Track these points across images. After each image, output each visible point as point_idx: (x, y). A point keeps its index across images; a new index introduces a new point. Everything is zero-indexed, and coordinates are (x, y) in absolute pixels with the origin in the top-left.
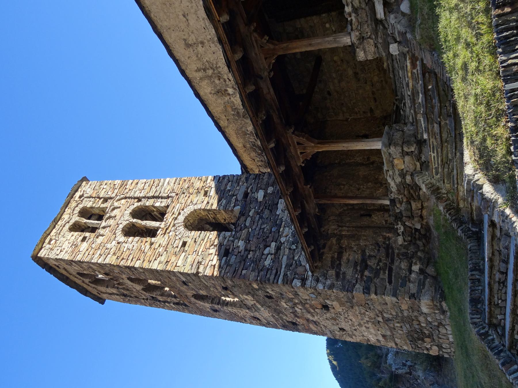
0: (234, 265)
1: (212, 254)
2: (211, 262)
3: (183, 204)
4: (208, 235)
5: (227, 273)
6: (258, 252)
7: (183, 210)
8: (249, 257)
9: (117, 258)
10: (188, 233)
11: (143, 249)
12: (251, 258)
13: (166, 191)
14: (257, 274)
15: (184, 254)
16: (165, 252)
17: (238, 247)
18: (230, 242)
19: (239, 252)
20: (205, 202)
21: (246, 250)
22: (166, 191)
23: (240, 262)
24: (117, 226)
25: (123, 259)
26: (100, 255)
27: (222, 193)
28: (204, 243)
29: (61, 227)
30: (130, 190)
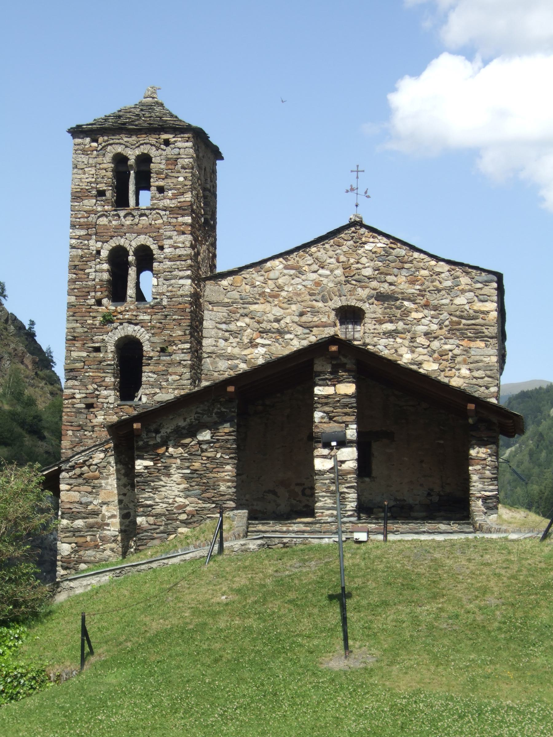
0: (76, 420)
1: (87, 389)
2: (77, 391)
3: (149, 324)
4: (109, 375)
5: (68, 416)
6: (91, 441)
7: (142, 327)
8: (86, 433)
9: (76, 266)
10: (111, 348)
11: (89, 297)
12: (85, 435)
13: (170, 288)
14: (68, 447)
15: (84, 354)
16: (86, 330)
17: (96, 416)
18: (101, 406)
19: (90, 420)
20: (151, 354)
21: (93, 427)
22: (170, 288)
23: (79, 426)
24: (123, 234)
25: (76, 274)
26: (80, 236)
27: (164, 373)
28: (99, 374)
29: (117, 141)
30: (174, 226)
